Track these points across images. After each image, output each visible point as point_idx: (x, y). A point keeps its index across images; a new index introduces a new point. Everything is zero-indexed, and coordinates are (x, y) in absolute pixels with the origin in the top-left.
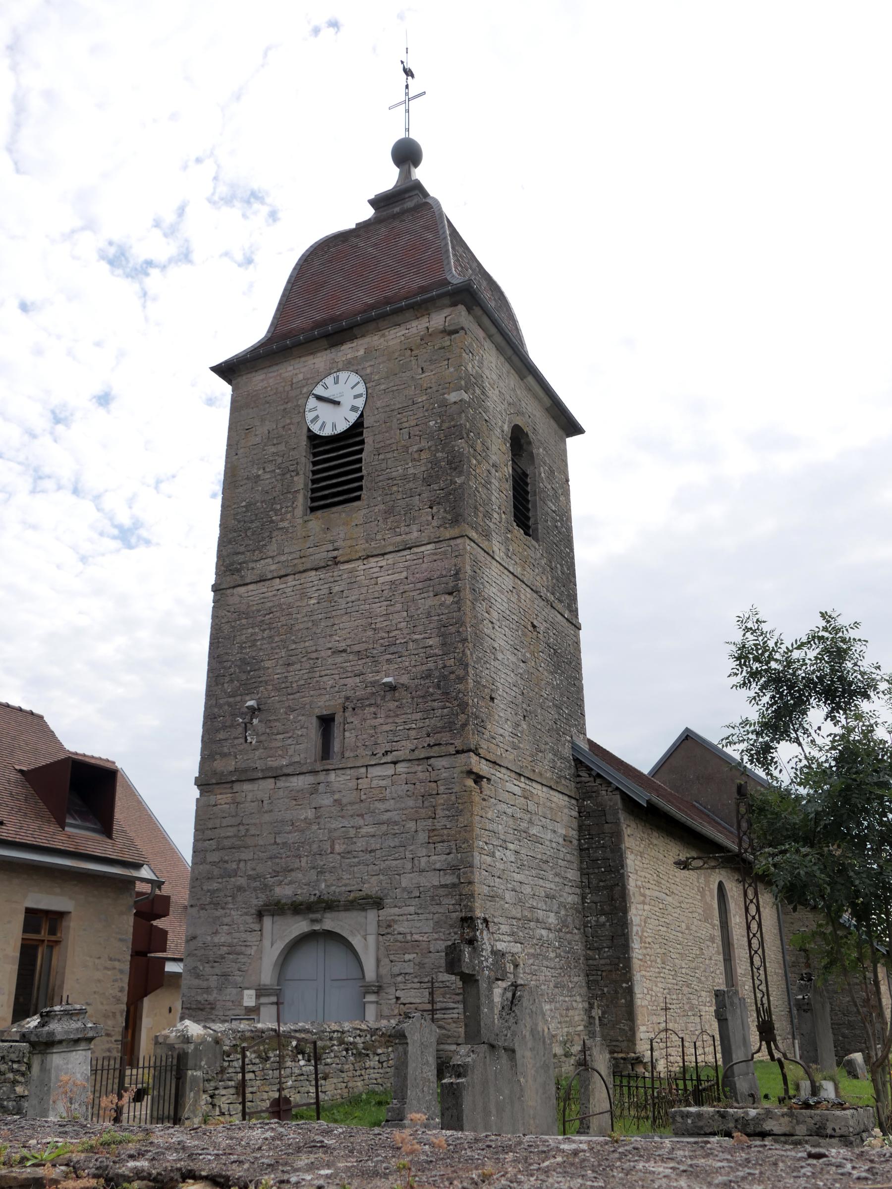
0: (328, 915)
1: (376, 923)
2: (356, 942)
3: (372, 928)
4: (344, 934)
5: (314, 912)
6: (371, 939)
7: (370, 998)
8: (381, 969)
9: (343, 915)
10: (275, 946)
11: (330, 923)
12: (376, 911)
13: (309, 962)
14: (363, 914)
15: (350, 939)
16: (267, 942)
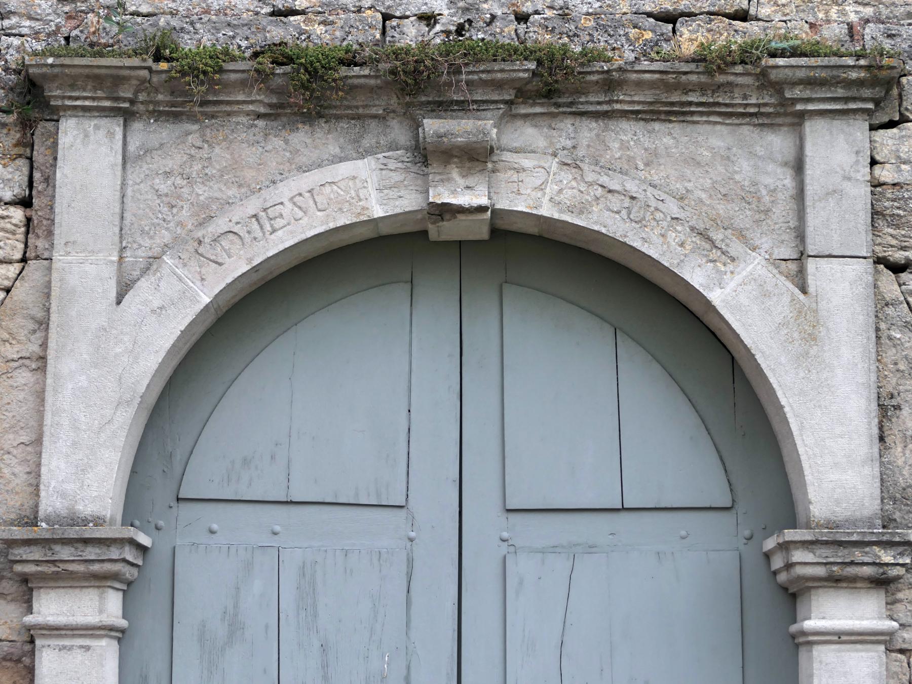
0: (528, 134)
1: (859, 195)
2: (740, 293)
3: (840, 216)
4: (661, 245)
5: (442, 107)
6: (843, 286)
7: (829, 613)
8: (898, 455)
9: (627, 138)
10: (144, 292)
11: (540, 176)
12: (859, 130)
13: (357, 397)
14: (778, 142)
15: (697, 275)
16: (82, 265)
